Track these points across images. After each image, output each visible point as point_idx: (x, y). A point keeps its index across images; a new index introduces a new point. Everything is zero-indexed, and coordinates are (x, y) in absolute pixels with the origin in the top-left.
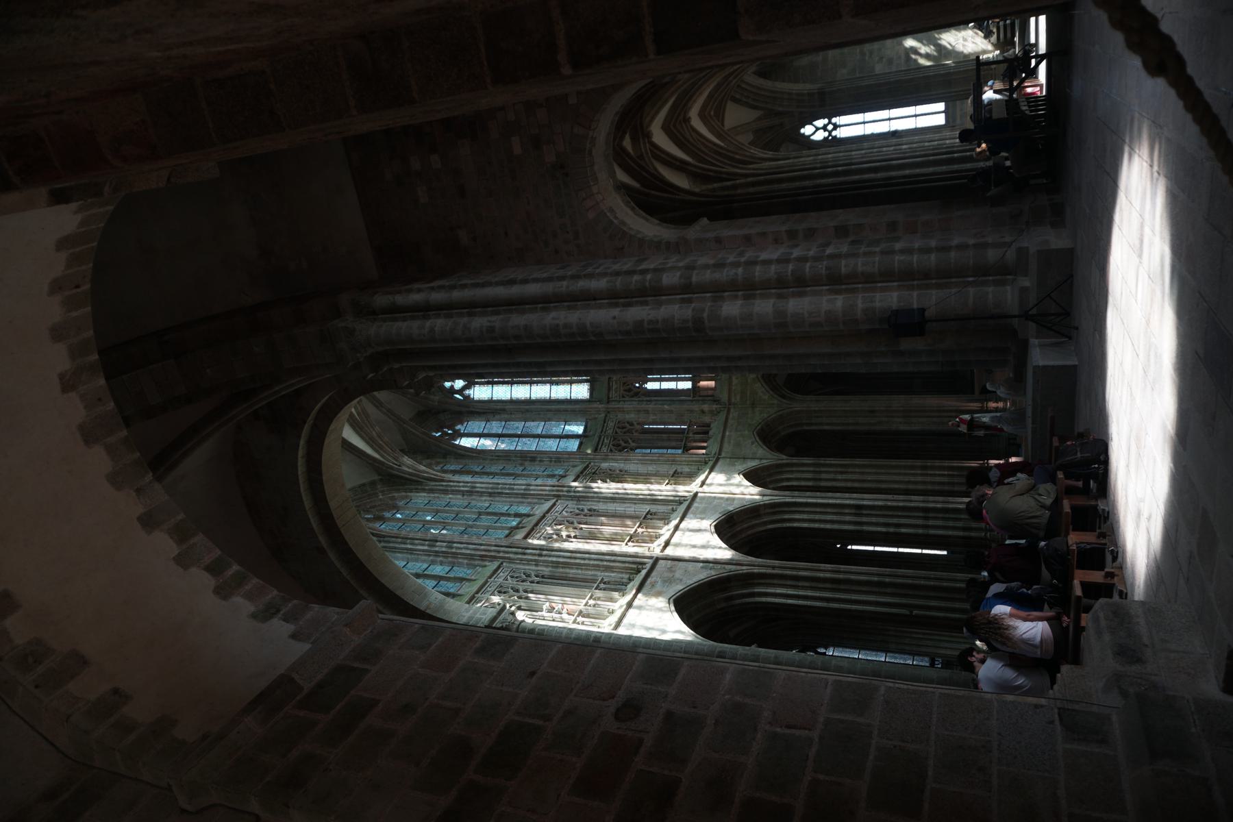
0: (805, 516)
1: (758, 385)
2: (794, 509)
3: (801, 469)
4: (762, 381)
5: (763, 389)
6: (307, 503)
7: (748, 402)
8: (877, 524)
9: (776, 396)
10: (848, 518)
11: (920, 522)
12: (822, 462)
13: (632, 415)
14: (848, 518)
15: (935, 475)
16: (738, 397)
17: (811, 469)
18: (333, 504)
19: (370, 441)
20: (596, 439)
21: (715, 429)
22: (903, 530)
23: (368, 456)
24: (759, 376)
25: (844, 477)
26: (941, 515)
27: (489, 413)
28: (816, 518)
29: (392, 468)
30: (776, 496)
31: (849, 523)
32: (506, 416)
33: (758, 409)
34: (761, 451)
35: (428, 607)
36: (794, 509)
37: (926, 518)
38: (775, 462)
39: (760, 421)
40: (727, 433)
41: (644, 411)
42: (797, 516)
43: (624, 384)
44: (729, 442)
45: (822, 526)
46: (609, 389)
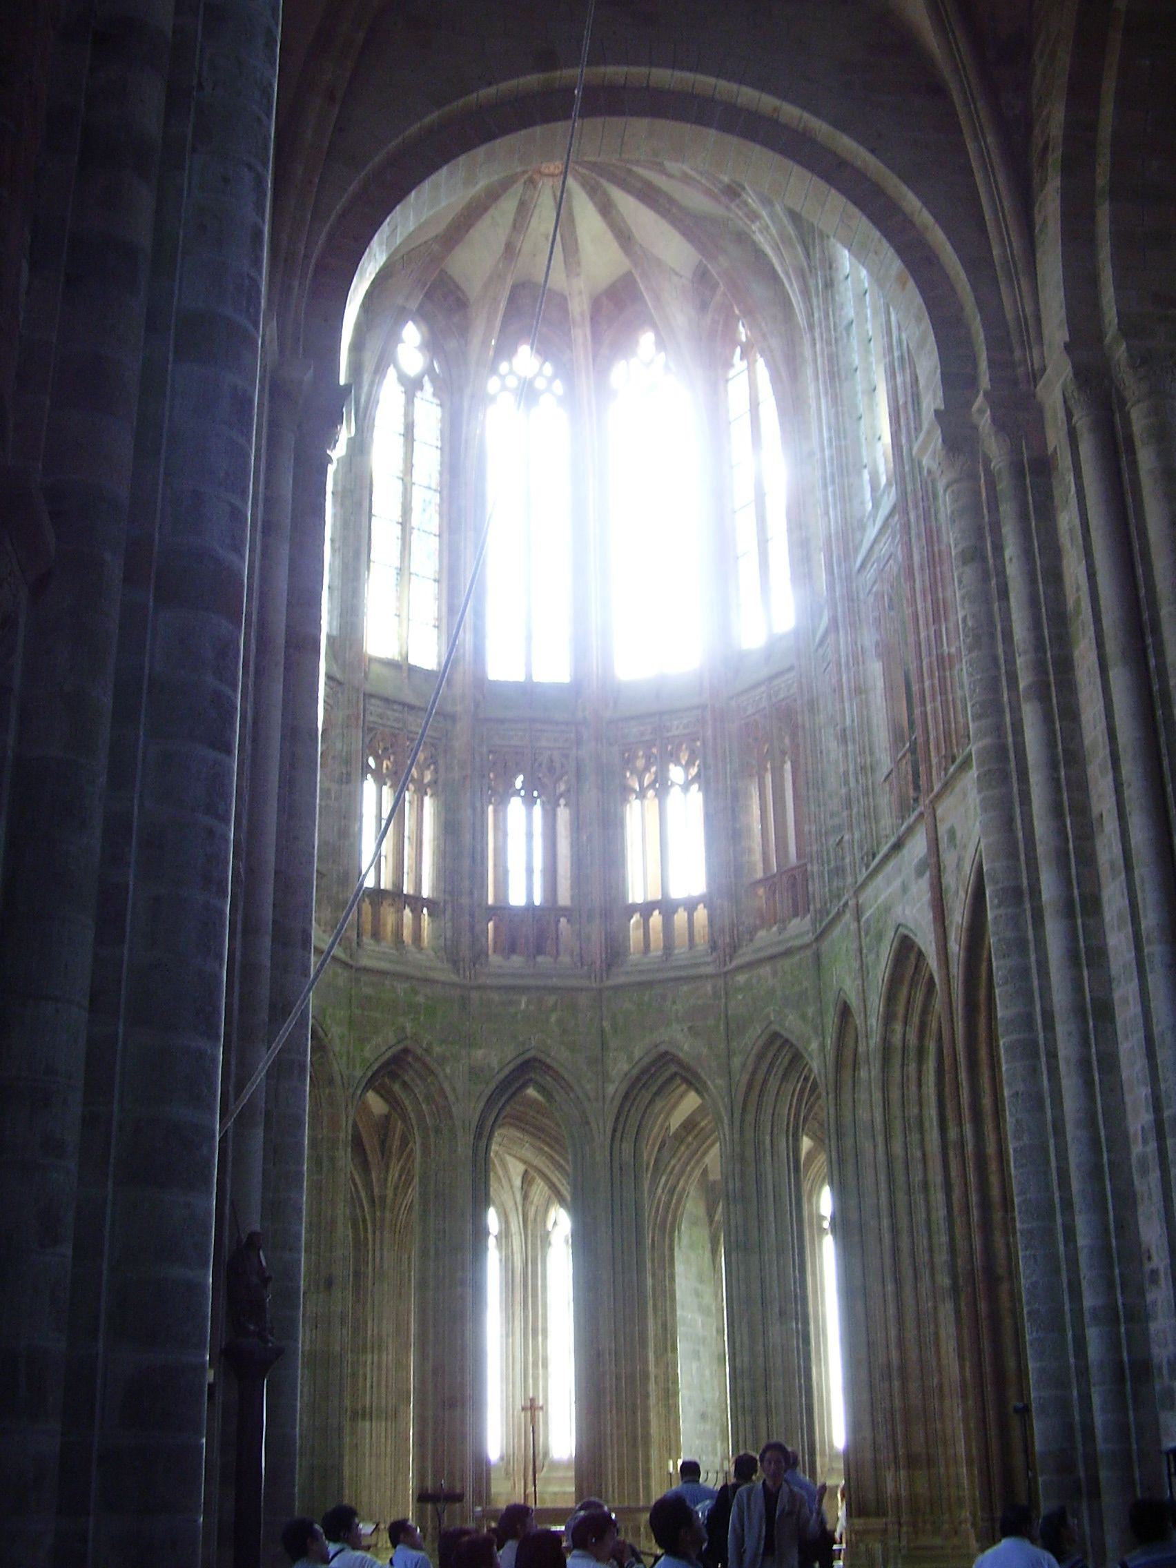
4: (400, 1047)
5: (384, 1049)
7: (358, 1012)
9: (370, 1074)
16: (368, 991)
24: (408, 1043)
46: (386, 700)
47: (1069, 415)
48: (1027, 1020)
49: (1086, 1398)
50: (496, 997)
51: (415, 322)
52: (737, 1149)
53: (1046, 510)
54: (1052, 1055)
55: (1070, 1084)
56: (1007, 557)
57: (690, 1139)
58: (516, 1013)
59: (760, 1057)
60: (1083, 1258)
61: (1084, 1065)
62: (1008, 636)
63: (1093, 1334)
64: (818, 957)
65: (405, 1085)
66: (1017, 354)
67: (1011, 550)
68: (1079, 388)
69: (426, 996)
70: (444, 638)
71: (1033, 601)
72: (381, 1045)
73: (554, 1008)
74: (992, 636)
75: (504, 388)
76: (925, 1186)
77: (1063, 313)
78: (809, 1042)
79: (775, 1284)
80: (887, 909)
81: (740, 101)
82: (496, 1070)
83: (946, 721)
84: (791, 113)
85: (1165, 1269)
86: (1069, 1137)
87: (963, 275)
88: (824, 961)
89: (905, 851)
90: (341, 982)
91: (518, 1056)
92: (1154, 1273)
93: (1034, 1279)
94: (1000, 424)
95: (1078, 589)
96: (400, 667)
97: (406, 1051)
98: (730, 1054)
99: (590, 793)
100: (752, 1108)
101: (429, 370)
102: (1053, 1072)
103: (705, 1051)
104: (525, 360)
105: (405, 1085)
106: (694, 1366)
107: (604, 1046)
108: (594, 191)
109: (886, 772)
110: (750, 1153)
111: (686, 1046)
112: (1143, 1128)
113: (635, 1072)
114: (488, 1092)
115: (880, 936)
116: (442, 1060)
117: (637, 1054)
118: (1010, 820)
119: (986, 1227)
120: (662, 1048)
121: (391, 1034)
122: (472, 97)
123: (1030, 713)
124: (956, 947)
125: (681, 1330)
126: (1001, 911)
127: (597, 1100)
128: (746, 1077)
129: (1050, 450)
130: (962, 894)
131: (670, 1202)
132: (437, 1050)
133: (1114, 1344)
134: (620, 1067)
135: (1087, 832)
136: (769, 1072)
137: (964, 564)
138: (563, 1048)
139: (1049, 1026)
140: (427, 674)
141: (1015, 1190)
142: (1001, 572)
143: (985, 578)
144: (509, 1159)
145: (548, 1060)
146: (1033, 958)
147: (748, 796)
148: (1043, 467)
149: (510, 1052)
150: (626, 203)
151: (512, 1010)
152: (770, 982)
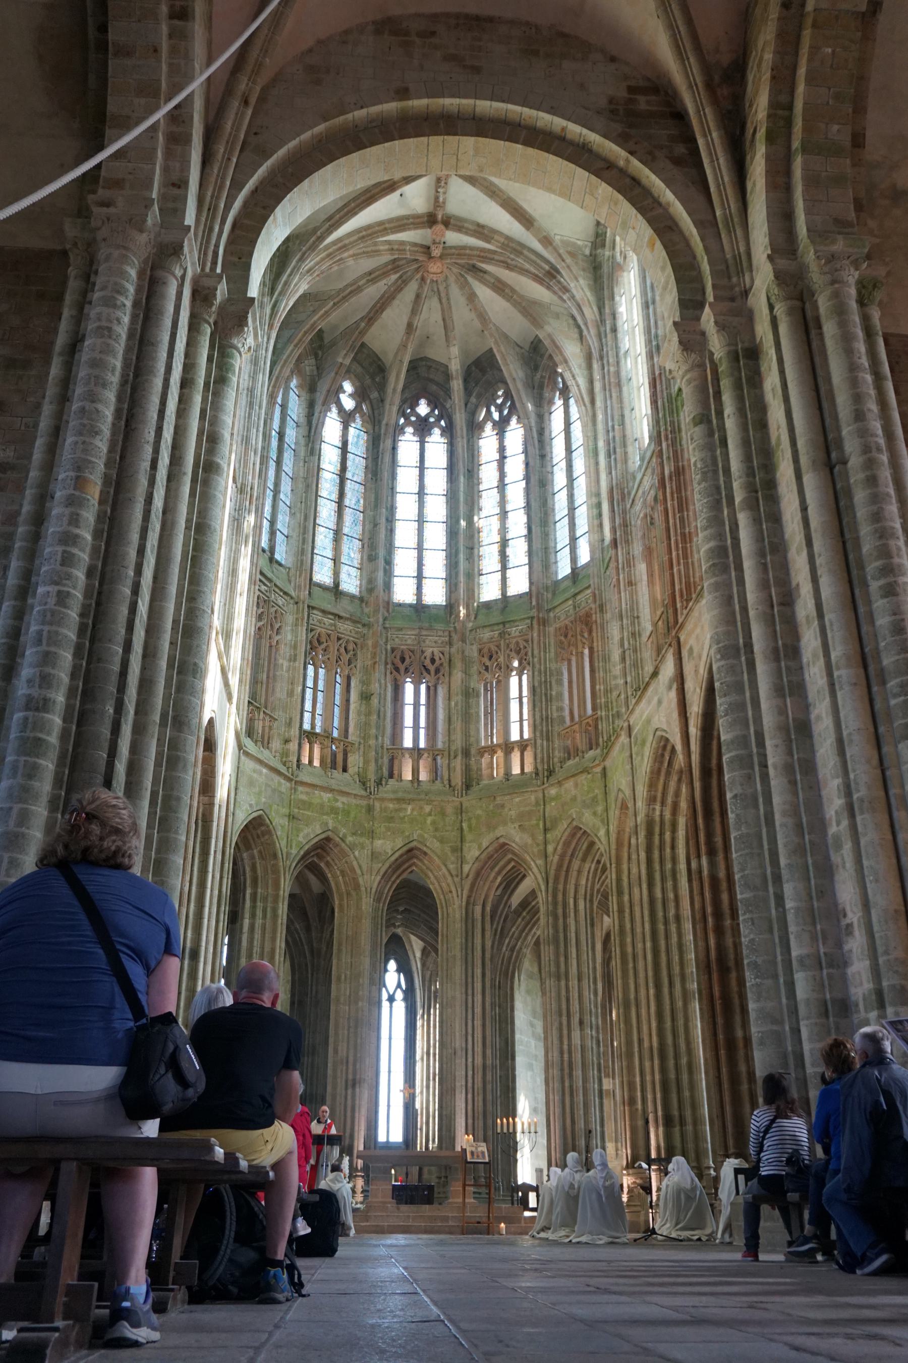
6: (486, 106)
9: (302, 853)
13: (289, 637)
16: (304, 797)
18: (469, 142)
19: (342, 245)
20: (269, 575)
21: (265, 755)
23: (329, 231)
24: (330, 833)
27: (310, 431)
29: (302, 259)
32: (302, 454)
34: (241, 818)
35: (275, 219)
40: (265, 771)
41: (295, 655)
43: (329, 636)
44: (254, 771)
46: (324, 612)
47: (771, 307)
48: (743, 741)
49: (796, 1031)
50: (391, 806)
51: (350, 379)
52: (551, 908)
53: (755, 380)
54: (764, 765)
55: (777, 782)
56: (726, 416)
57: (524, 914)
59: (567, 844)
60: (790, 917)
61: (788, 769)
62: (727, 471)
63: (800, 978)
64: (604, 769)
66: (734, 280)
67: (729, 409)
68: (779, 285)
70: (364, 574)
71: (746, 443)
72: (309, 834)
73: (430, 814)
74: (715, 472)
75: (408, 423)
76: (678, 918)
77: (767, 240)
78: (598, 830)
79: (577, 1002)
80: (648, 721)
81: (540, 124)
83: (687, 576)
84: (575, 130)
85: (859, 921)
86: (777, 823)
87: (694, 231)
88: (609, 774)
89: (660, 676)
90: (283, 790)
92: (849, 926)
93: (752, 936)
94: (721, 326)
95: (779, 428)
96: (335, 590)
97: (328, 839)
98: (546, 843)
99: (458, 676)
100: (562, 880)
101: (358, 408)
102: (765, 777)
103: (530, 841)
104: (423, 409)
106: (529, 1073)
107: (462, 840)
108: (464, 285)
109: (648, 634)
110: (560, 911)
111: (517, 838)
112: (836, 812)
113: (483, 856)
115: (644, 742)
116: (352, 847)
117: (485, 845)
118: (730, 597)
119: (719, 930)
120: (502, 840)
122: (350, 116)
123: (743, 518)
124: (694, 731)
125: (519, 1048)
126: (723, 663)
128: (557, 857)
129: (758, 340)
130: (698, 690)
131: (511, 957)
132: (350, 839)
133: (819, 986)
134: (472, 852)
135: (788, 599)
136: (572, 855)
137: (695, 425)
139: (761, 743)
140: (352, 597)
141: (736, 869)
142: (722, 428)
143: (711, 434)
144: (413, 938)
145: (425, 849)
146: (748, 694)
147: (559, 673)
148: (753, 353)
149: (399, 842)
150: (484, 293)
151: (401, 815)
152: (573, 792)
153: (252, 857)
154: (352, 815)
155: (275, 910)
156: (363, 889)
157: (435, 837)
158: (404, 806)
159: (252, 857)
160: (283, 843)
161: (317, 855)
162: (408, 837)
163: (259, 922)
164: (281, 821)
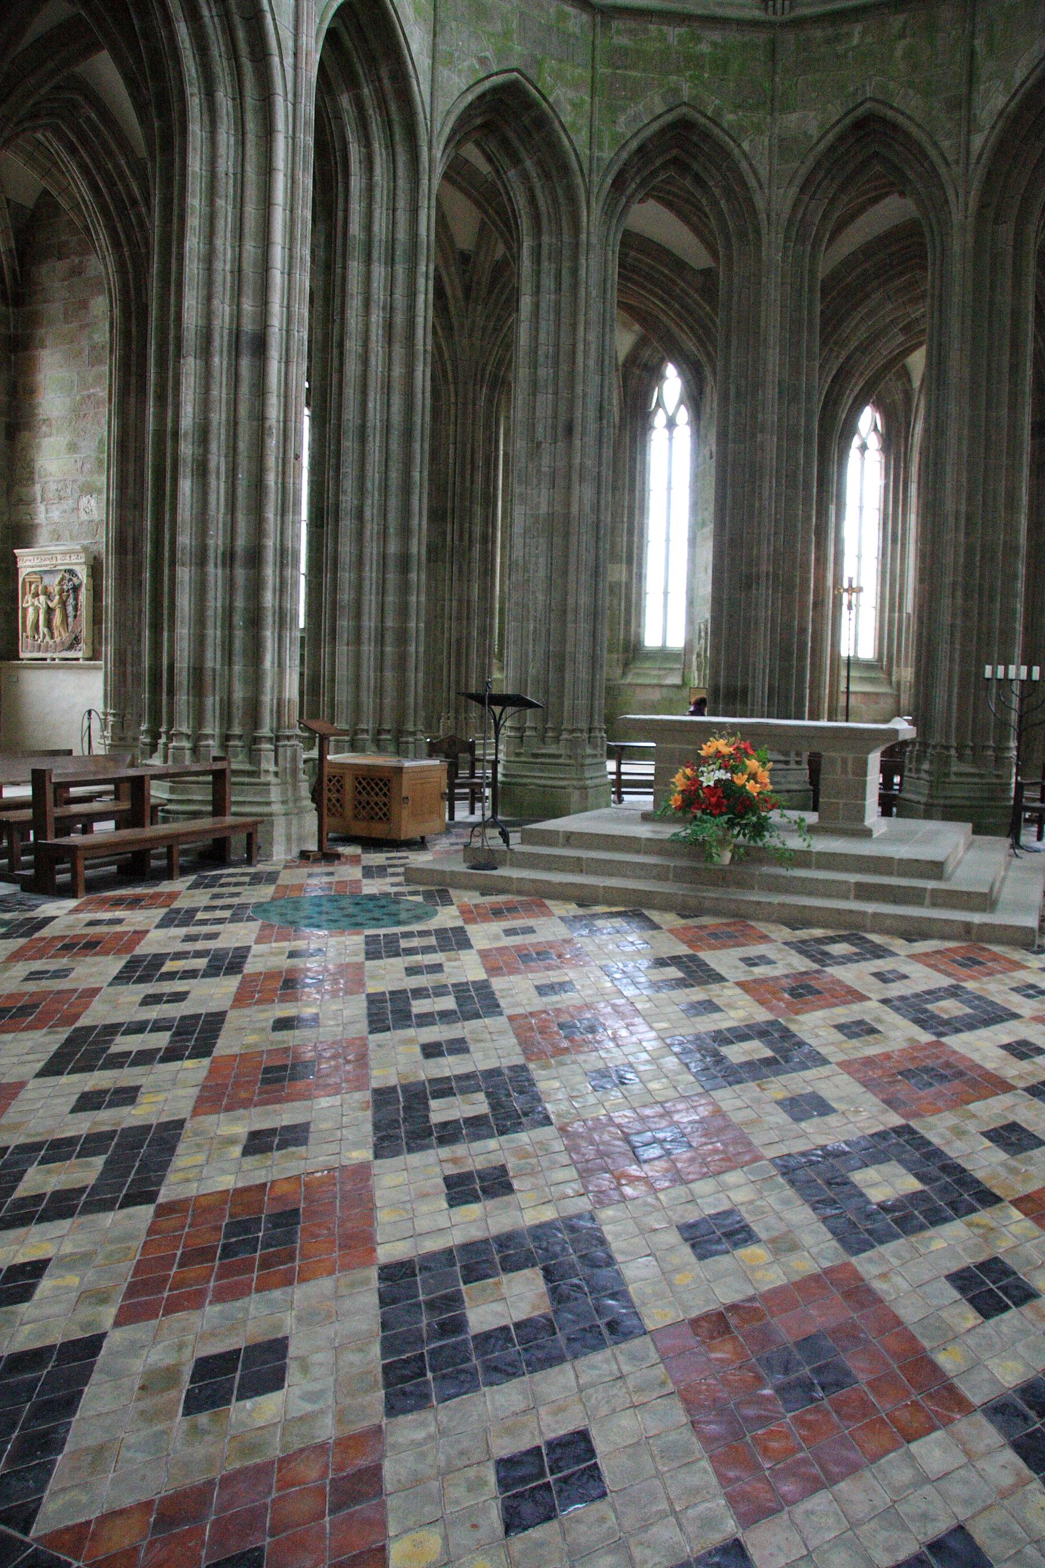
0: (226, 164)
1: (659, 108)
2: (251, 126)
3: (402, 203)
4: (669, 118)
8: (205, 404)
9: (625, 155)
10: (223, 309)
11: (216, 541)
12: (422, 268)
14: (223, 309)
15: (383, 591)
16: (624, 41)
17: (402, 235)
22: (186, 486)
24: (684, 110)
25: (377, 332)
26: (239, 603)
28: (220, 202)
30: (296, 68)
31: (208, 314)
33: (587, 99)
36: (251, 126)
37: (229, 558)
38: (421, 117)
39: (551, 100)
42: (226, 137)
45: (194, 222)
50: (818, 34)
58: (846, 51)
65: (698, 180)
69: (715, 45)
82: (815, 139)
91: (846, 114)
105: (698, 180)
114: (804, 171)
121: (657, 100)
127: (957, 162)
132: (730, 118)
138: (911, 92)
145: (890, 113)
149: (835, 110)
151: (840, 49)
153: (525, 177)
154: (734, 67)
155: (575, 271)
156: (763, 216)
157: (910, 84)
158: (845, 29)
159: (525, 177)
160: (581, 139)
161: (675, 161)
162: (854, 94)
163: (547, 299)
164: (571, 94)
